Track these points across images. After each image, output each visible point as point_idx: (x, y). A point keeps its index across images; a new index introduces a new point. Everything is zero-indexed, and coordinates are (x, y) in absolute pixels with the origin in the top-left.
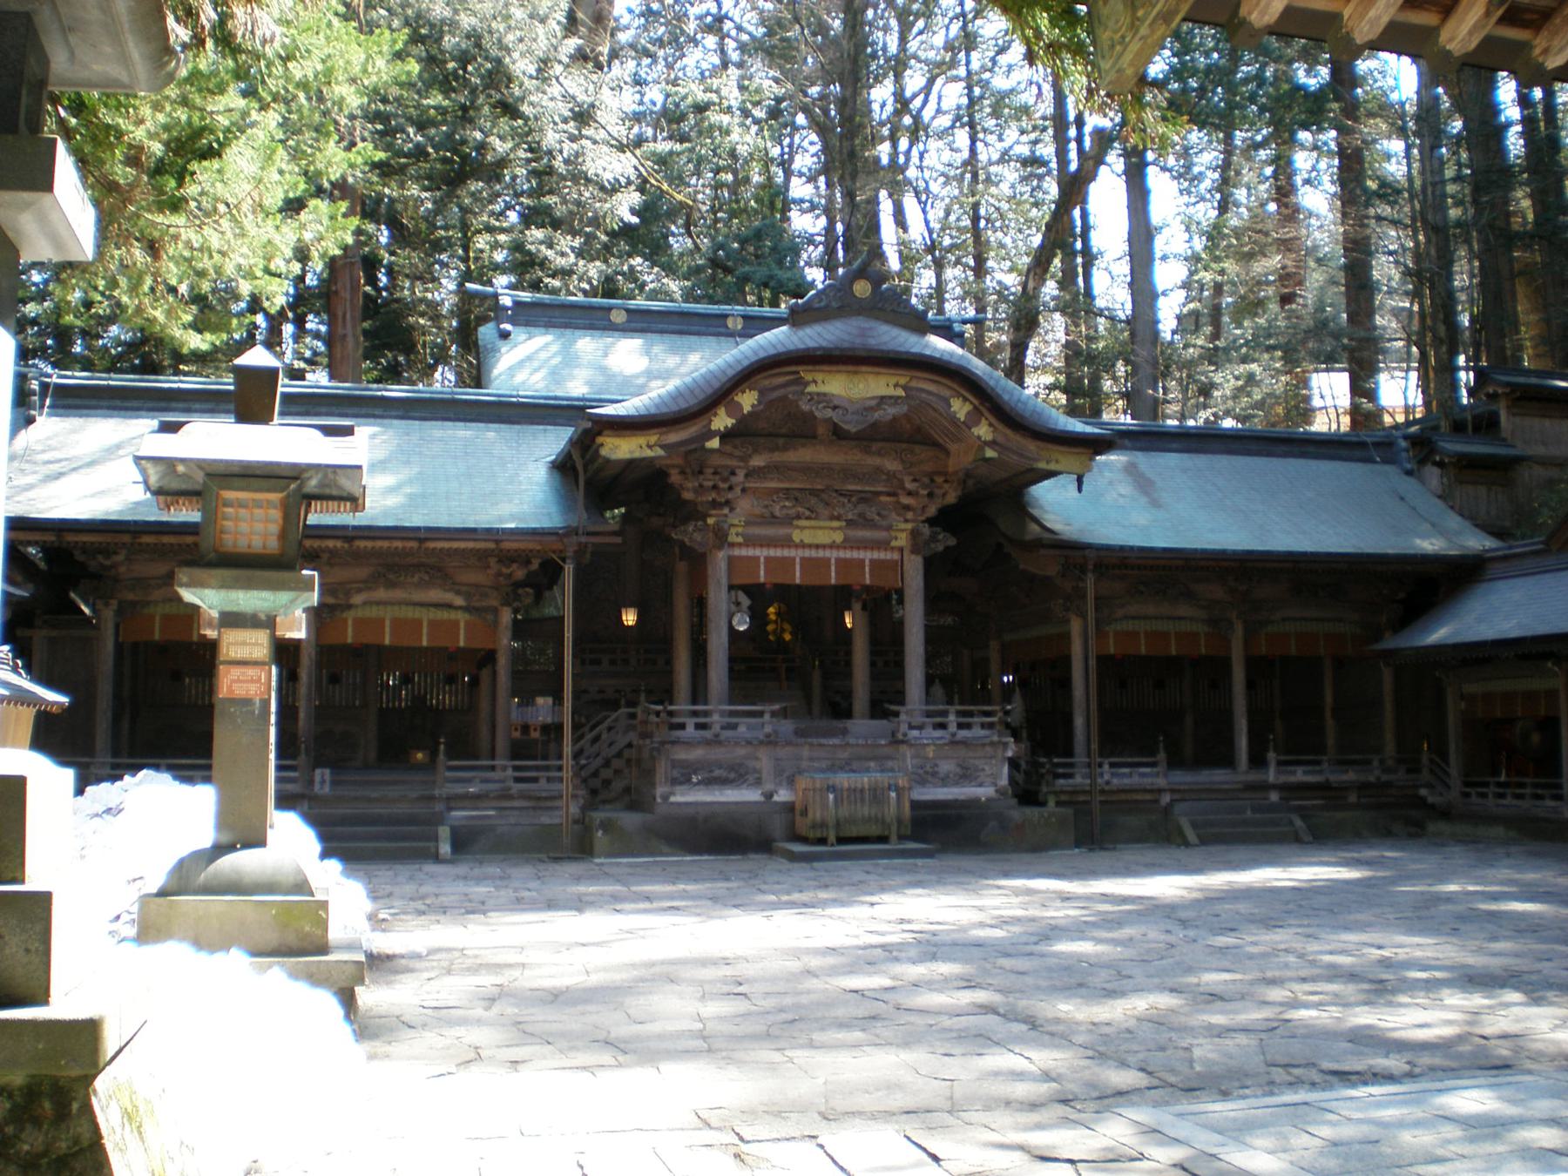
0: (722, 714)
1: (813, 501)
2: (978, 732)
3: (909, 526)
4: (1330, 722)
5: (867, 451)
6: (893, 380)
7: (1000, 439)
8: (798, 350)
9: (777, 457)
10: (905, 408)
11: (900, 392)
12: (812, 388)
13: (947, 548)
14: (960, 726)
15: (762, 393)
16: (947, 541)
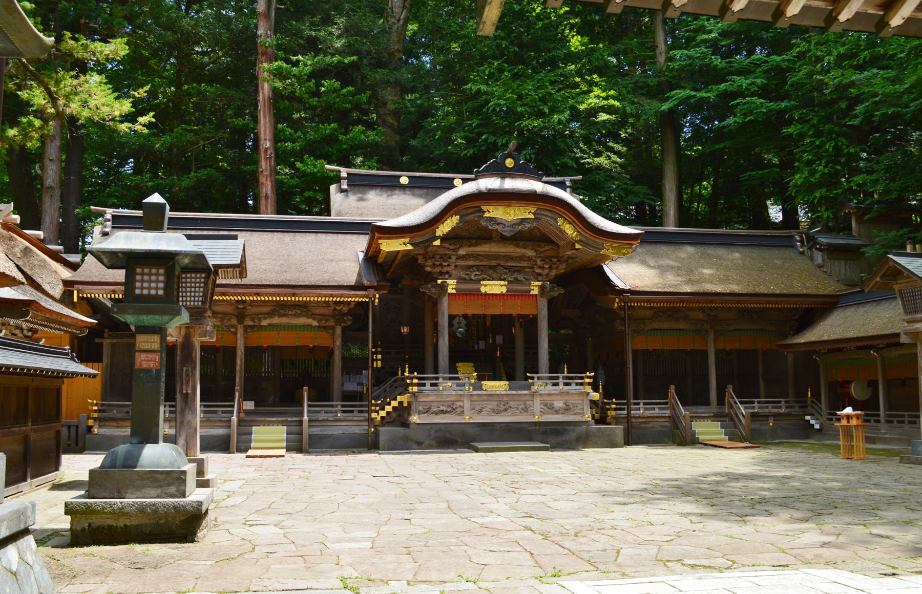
1: (491, 272)
2: (573, 387)
3: (540, 283)
4: (761, 383)
5: (518, 246)
7: (583, 239)
9: (472, 249)
11: (532, 216)
12: (487, 215)
13: (559, 295)
15: (461, 217)
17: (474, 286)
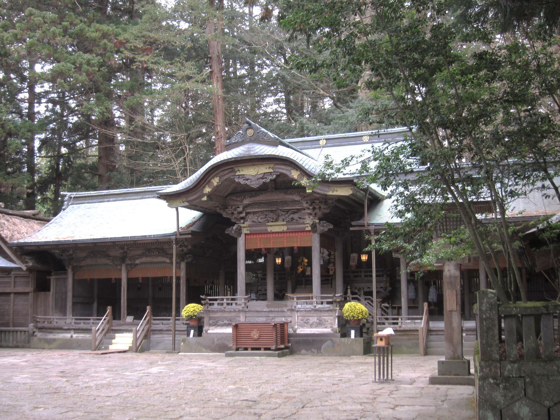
0: (228, 299)
2: (326, 306)
6: (268, 167)
8: (225, 160)
10: (274, 176)
11: (271, 170)
12: (238, 173)
13: (329, 230)
14: (228, 304)
16: (326, 227)
17: (264, 228)
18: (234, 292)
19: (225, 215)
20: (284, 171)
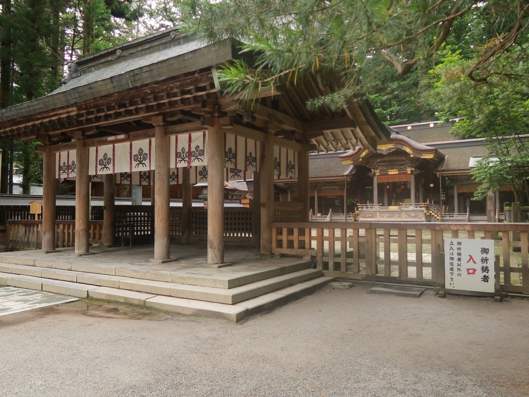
2: (418, 208)
16: (418, 172)
18: (372, 201)
19: (368, 167)
20: (400, 147)
